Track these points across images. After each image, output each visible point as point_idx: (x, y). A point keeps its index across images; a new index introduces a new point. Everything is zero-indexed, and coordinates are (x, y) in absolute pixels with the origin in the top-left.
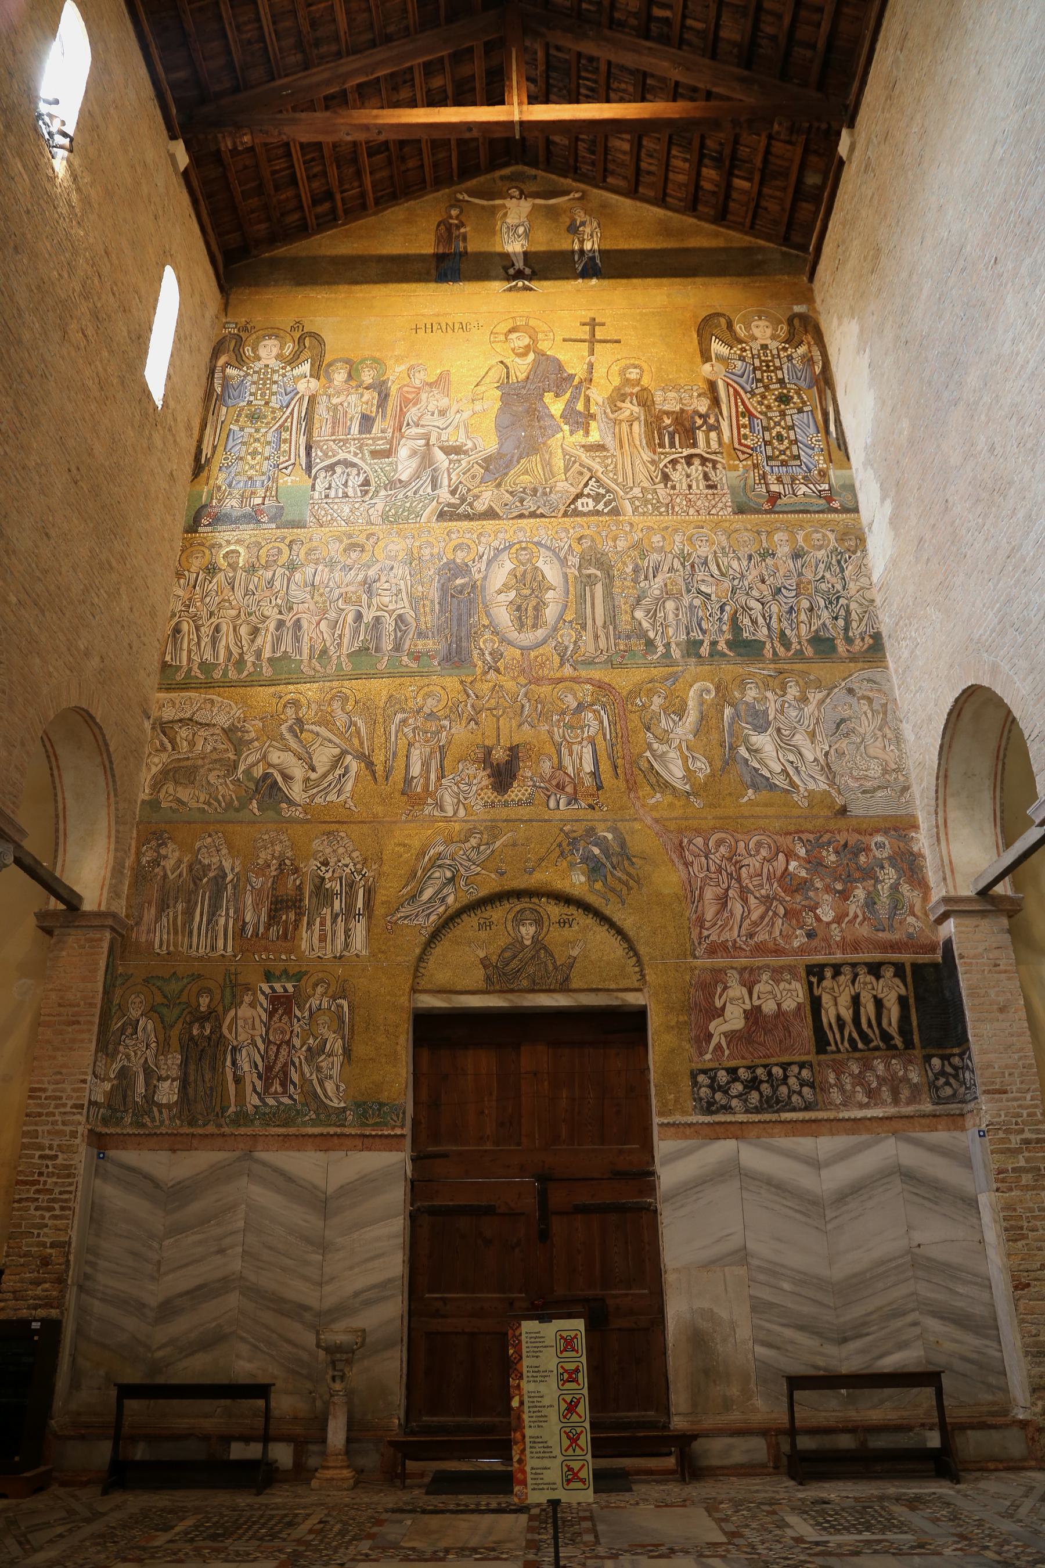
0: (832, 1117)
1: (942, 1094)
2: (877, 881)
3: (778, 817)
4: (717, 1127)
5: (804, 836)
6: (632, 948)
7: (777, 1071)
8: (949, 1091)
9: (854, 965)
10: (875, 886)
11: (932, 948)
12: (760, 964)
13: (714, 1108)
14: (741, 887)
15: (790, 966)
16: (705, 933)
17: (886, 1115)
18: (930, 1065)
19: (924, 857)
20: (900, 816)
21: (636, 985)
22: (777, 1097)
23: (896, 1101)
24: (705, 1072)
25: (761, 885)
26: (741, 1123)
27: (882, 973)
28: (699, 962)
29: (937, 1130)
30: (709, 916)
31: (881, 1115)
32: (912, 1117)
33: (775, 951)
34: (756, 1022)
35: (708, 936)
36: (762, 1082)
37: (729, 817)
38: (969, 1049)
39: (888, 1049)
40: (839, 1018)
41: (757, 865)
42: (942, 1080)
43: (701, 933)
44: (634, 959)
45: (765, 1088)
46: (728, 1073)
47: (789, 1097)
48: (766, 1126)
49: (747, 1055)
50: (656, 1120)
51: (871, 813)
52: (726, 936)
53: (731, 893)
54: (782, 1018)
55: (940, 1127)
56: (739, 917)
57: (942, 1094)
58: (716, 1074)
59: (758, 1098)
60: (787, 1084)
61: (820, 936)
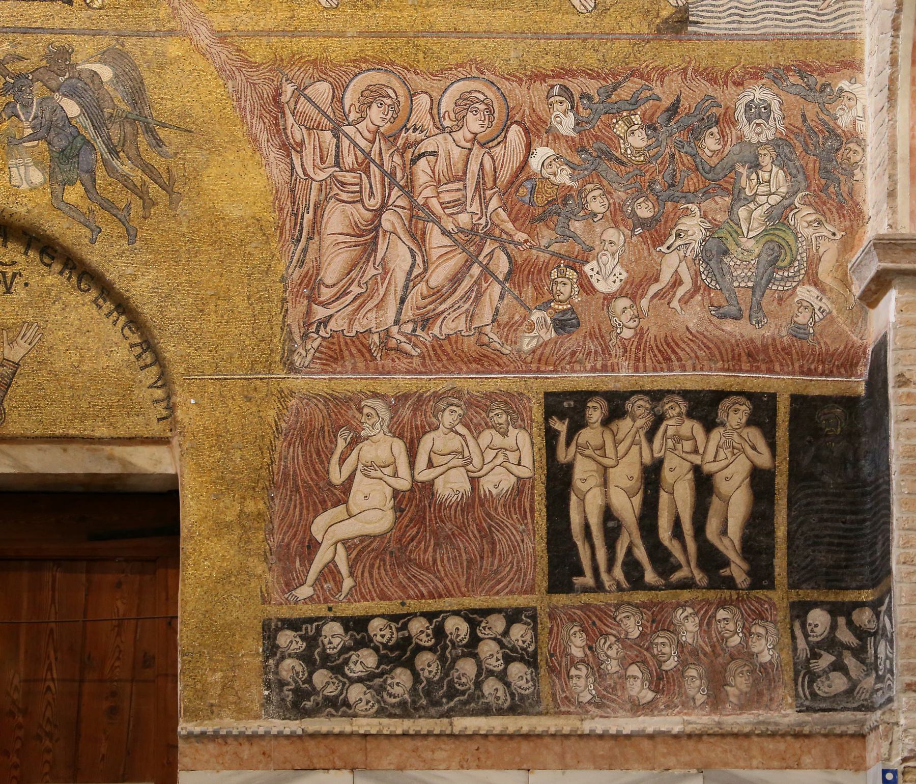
0: (567, 730)
1: (822, 688)
2: (738, 197)
3: (517, 36)
4: (311, 744)
5: (576, 86)
6: (149, 345)
7: (457, 627)
8: (839, 683)
9: (657, 396)
10: (731, 210)
11: (848, 364)
12: (440, 388)
13: (309, 704)
14: (413, 205)
15: (509, 394)
16: (320, 313)
17: (689, 729)
18: (803, 626)
19: (860, 142)
20: (819, 37)
21: (157, 429)
22: (451, 684)
23: (716, 700)
24: (293, 625)
25: (460, 204)
26: (365, 736)
27: (721, 416)
28: (298, 382)
29: (799, 766)
30: (331, 274)
31: (676, 729)
32: (747, 736)
33: (478, 361)
34: (419, 519)
35: (325, 322)
36: (419, 649)
37: (401, 34)
38: (889, 590)
39: (711, 587)
40: (608, 514)
41: (457, 153)
42: (827, 659)
43: (309, 312)
44: (155, 369)
45: (427, 663)
46: (347, 630)
47: (478, 684)
48: (419, 743)
49: (391, 590)
50: (184, 726)
51: (746, 29)
52: (367, 321)
53: (388, 220)
54: (479, 512)
55: (807, 760)
56: (400, 278)
57: (822, 688)
58: (319, 630)
59: (409, 685)
60: (475, 656)
61: (585, 328)
